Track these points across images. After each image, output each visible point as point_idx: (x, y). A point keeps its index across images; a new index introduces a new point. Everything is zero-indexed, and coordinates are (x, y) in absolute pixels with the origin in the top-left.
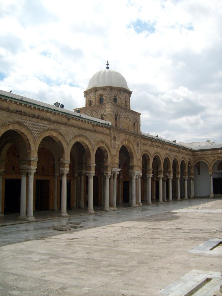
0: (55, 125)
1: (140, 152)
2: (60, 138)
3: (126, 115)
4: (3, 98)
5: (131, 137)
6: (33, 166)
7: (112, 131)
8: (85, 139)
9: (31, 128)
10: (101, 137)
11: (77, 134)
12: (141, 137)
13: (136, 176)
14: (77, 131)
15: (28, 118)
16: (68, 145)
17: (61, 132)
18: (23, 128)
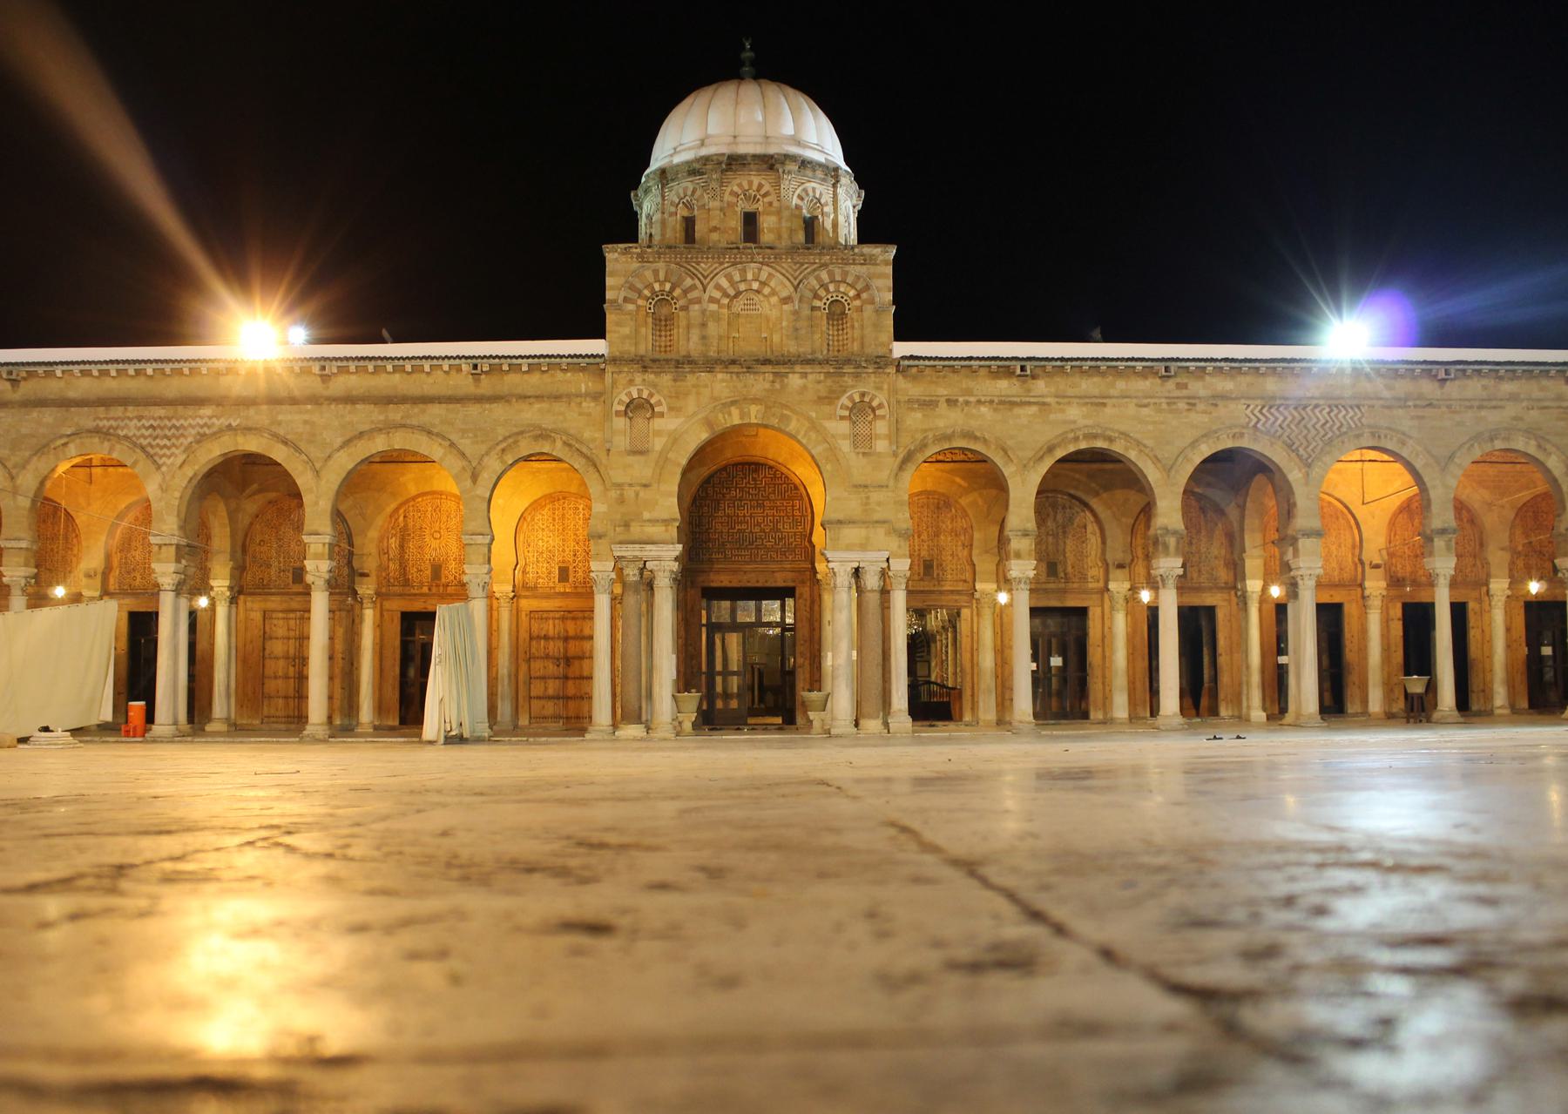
0: (252, 411)
1: (881, 446)
2: (279, 454)
3: (744, 280)
4: (40, 370)
5: (795, 381)
6: (159, 561)
7: (608, 377)
8: (424, 438)
9: (144, 442)
10: (531, 414)
11: (366, 427)
12: (892, 370)
13: (857, 572)
14: (365, 416)
15: (132, 411)
16: (317, 473)
17: (282, 432)
18: (118, 447)
